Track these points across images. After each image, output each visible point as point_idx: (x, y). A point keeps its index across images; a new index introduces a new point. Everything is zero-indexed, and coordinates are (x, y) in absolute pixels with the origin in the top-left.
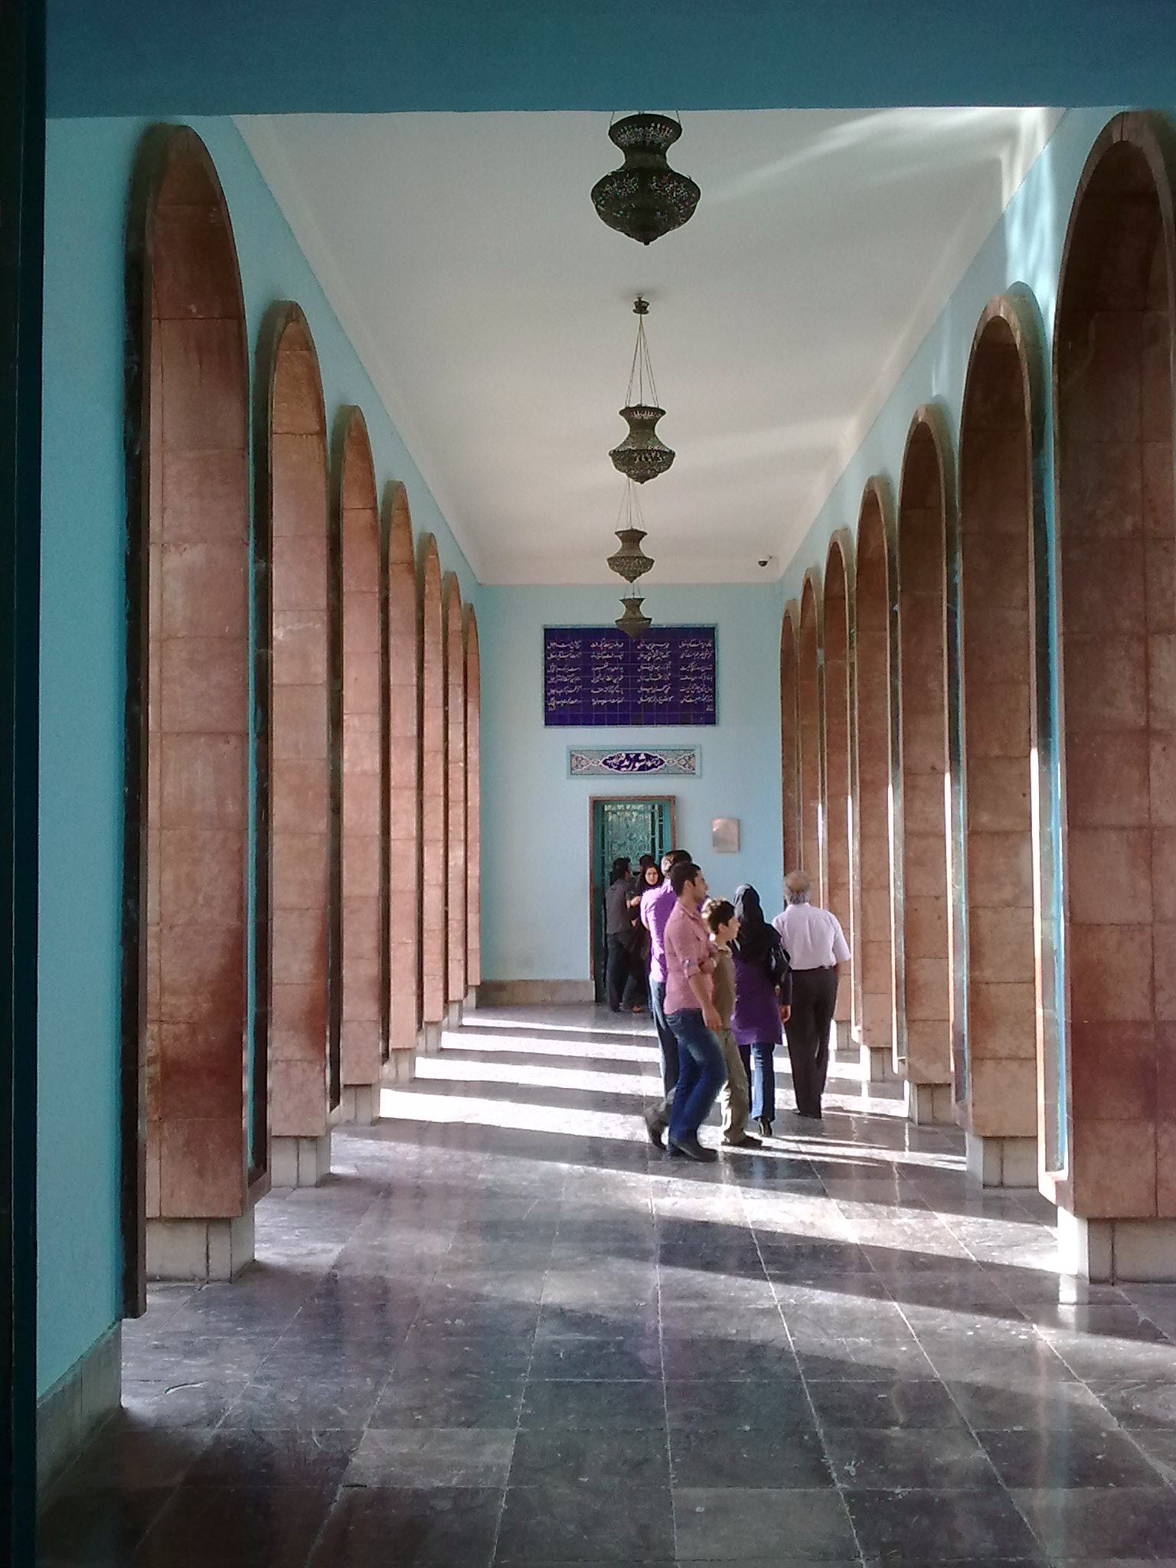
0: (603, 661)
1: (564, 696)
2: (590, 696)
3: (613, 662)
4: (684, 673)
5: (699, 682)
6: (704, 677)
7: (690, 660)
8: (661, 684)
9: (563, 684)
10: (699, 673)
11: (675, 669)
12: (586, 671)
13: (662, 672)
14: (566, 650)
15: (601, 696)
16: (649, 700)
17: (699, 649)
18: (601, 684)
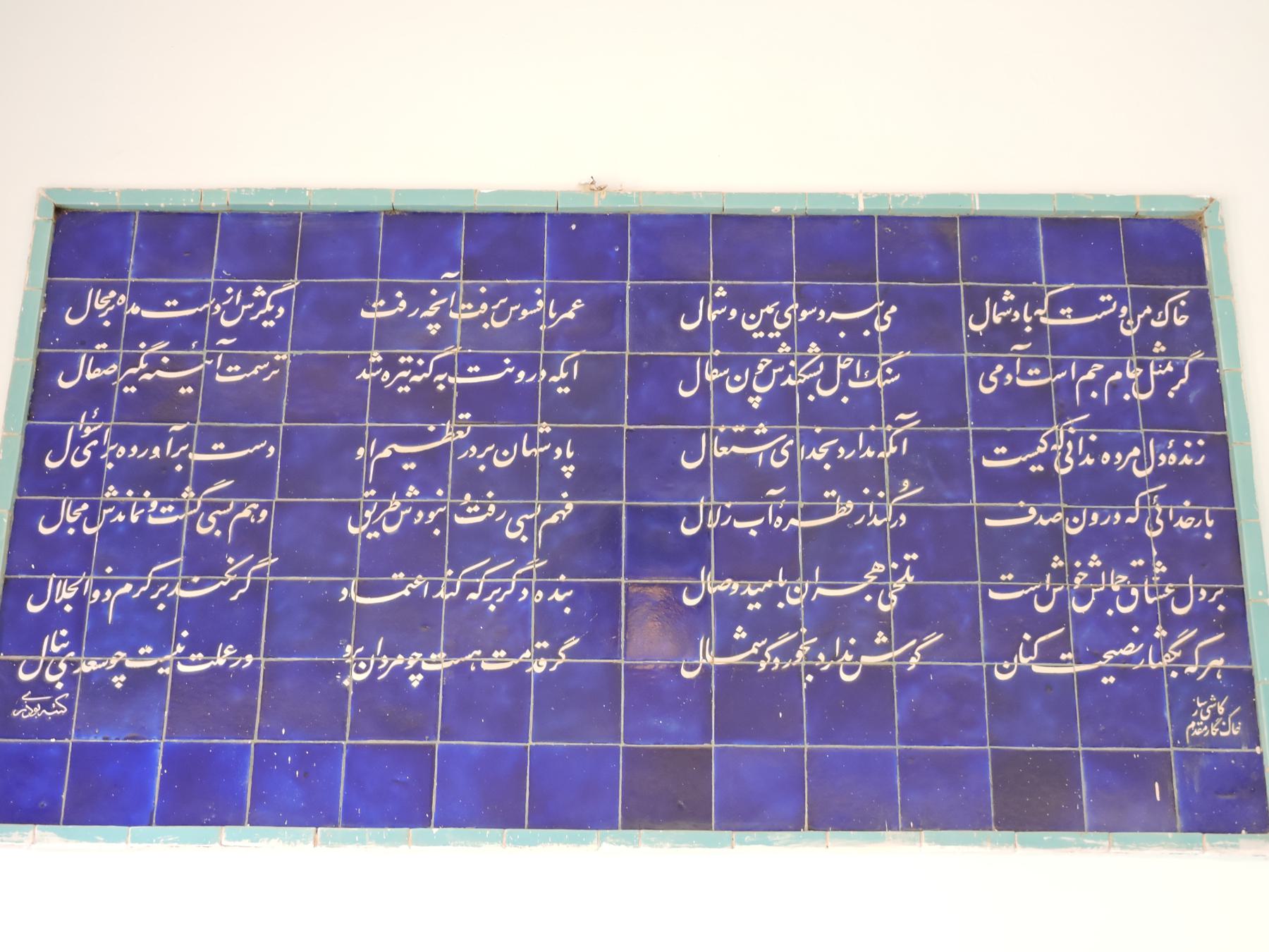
0: (431, 404)
1: (142, 624)
2: (332, 620)
3: (500, 408)
4: (996, 485)
5: (1120, 546)
6: (1153, 516)
7: (1036, 406)
8: (841, 551)
9: (138, 546)
10: (1117, 488)
11: (935, 461)
12: (318, 466)
13: (853, 477)
14: (180, 334)
15: (413, 622)
16: (766, 656)
17: (1105, 340)
18: (416, 550)
